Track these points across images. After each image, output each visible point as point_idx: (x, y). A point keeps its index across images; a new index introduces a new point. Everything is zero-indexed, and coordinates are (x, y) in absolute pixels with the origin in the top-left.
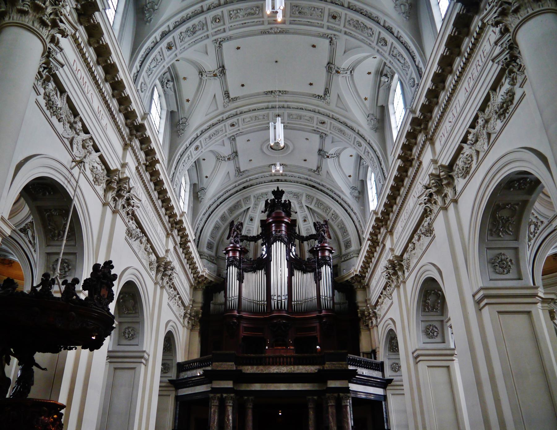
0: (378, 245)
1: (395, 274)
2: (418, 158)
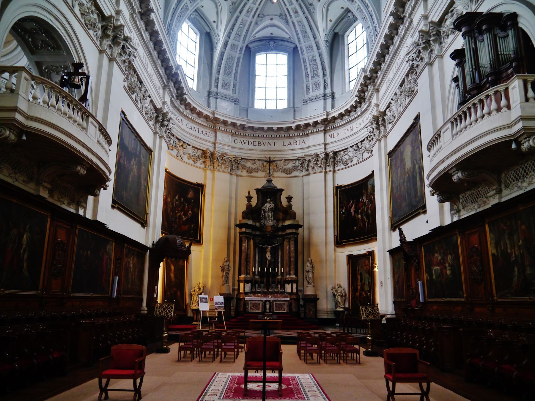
0: (364, 102)
1: (378, 128)
2: (410, 16)
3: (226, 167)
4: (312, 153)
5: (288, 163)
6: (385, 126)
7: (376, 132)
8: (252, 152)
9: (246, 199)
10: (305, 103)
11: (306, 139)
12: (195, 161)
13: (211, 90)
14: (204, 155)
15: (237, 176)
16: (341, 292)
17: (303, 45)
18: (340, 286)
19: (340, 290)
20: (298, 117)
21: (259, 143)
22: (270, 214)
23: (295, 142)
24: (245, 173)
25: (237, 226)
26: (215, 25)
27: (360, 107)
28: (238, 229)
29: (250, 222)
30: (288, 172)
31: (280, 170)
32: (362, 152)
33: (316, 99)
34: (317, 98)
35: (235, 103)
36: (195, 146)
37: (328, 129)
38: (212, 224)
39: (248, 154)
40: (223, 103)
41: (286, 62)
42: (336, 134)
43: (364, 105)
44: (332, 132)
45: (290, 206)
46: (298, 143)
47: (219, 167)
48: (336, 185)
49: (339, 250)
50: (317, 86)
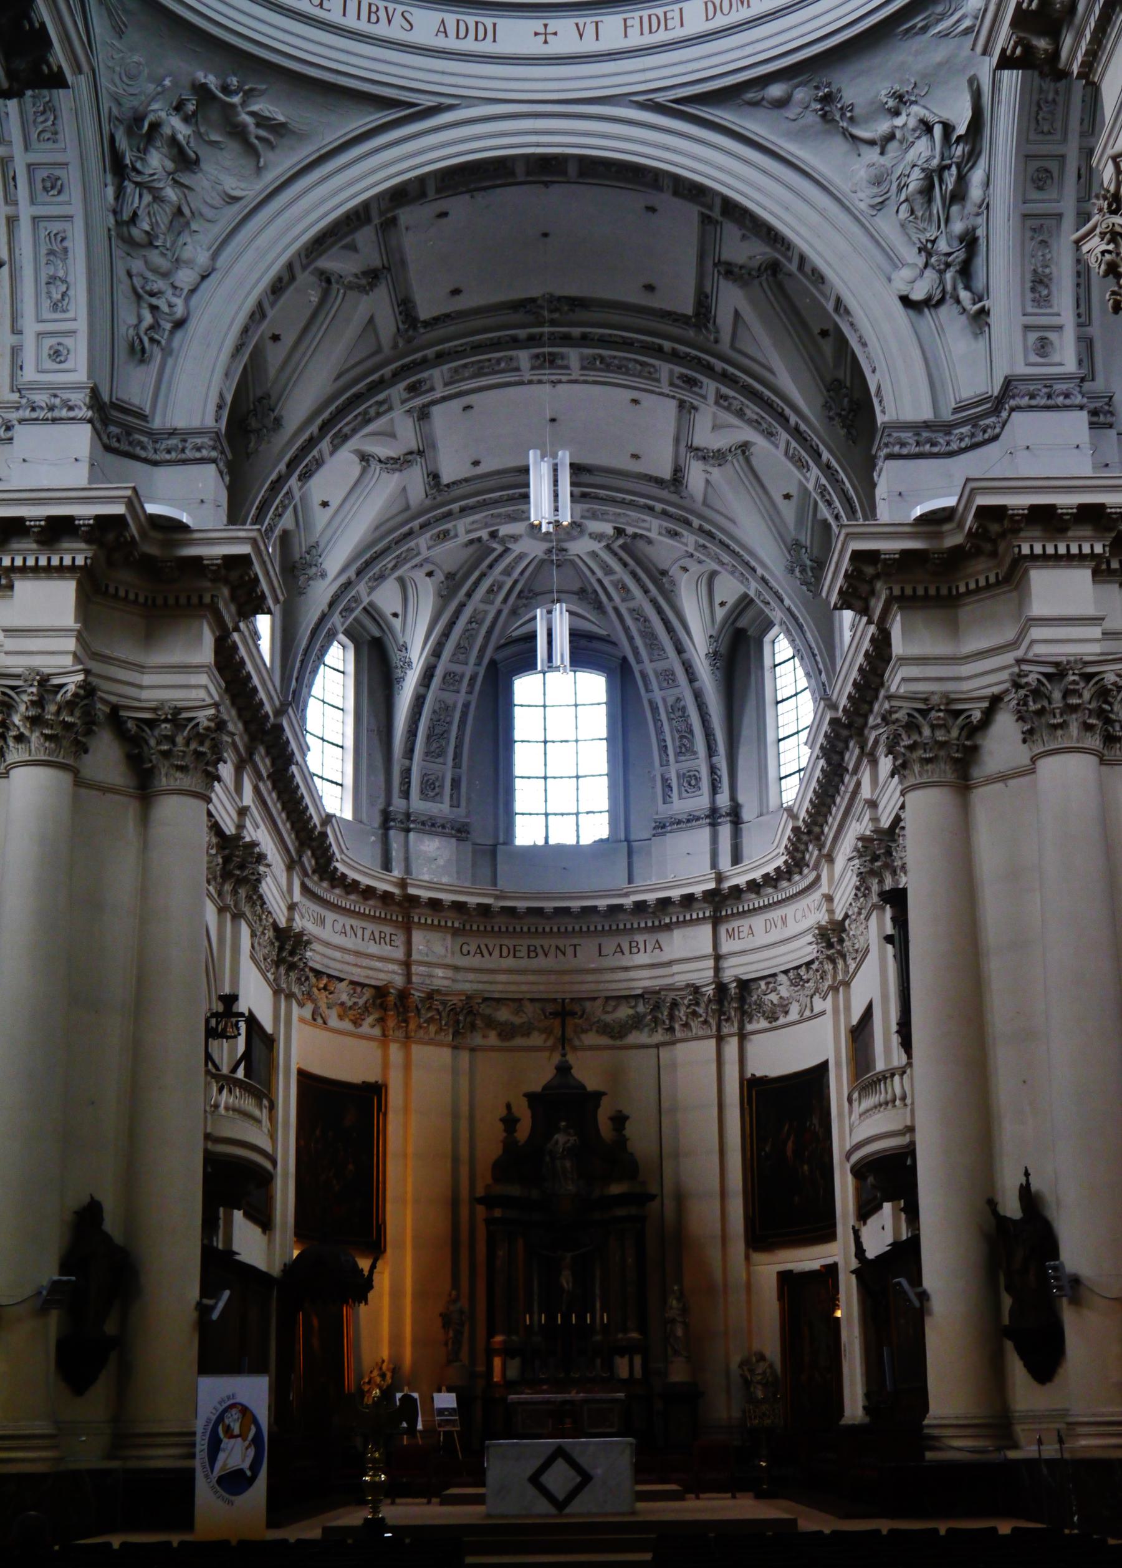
3: (441, 1029)
4: (680, 980)
5: (615, 1008)
6: (844, 956)
7: (829, 967)
8: (514, 978)
9: (500, 1126)
10: (660, 831)
11: (663, 937)
12: (356, 1023)
13: (391, 809)
14: (379, 1001)
15: (473, 1050)
16: (764, 1373)
17: (649, 668)
18: (762, 1357)
19: (761, 1367)
20: (639, 882)
21: (532, 948)
22: (568, 1164)
23: (634, 944)
24: (493, 1039)
25: (480, 1201)
26: (397, 623)
27: (801, 873)
28: (481, 1210)
29: (515, 1190)
30: (616, 1032)
31: (594, 1028)
32: (810, 993)
33: (688, 821)
34: (692, 819)
35: (459, 839)
36: (356, 979)
37: (724, 913)
38: (409, 1196)
39: (501, 984)
40: (427, 843)
41: (603, 698)
42: (746, 929)
43: (800, 882)
44: (735, 924)
45: (621, 1141)
46: (642, 949)
47: (422, 1032)
48: (749, 1076)
49: (757, 1257)
50: (690, 781)
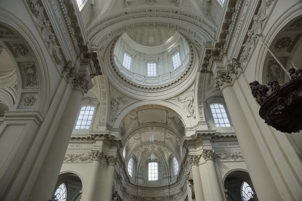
34: (166, 178)
50: (166, 173)
